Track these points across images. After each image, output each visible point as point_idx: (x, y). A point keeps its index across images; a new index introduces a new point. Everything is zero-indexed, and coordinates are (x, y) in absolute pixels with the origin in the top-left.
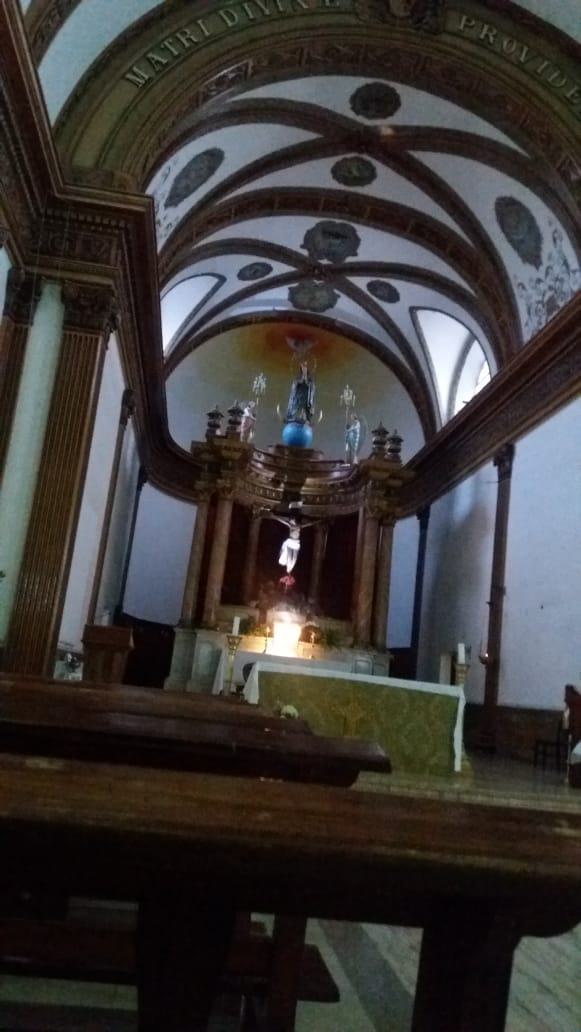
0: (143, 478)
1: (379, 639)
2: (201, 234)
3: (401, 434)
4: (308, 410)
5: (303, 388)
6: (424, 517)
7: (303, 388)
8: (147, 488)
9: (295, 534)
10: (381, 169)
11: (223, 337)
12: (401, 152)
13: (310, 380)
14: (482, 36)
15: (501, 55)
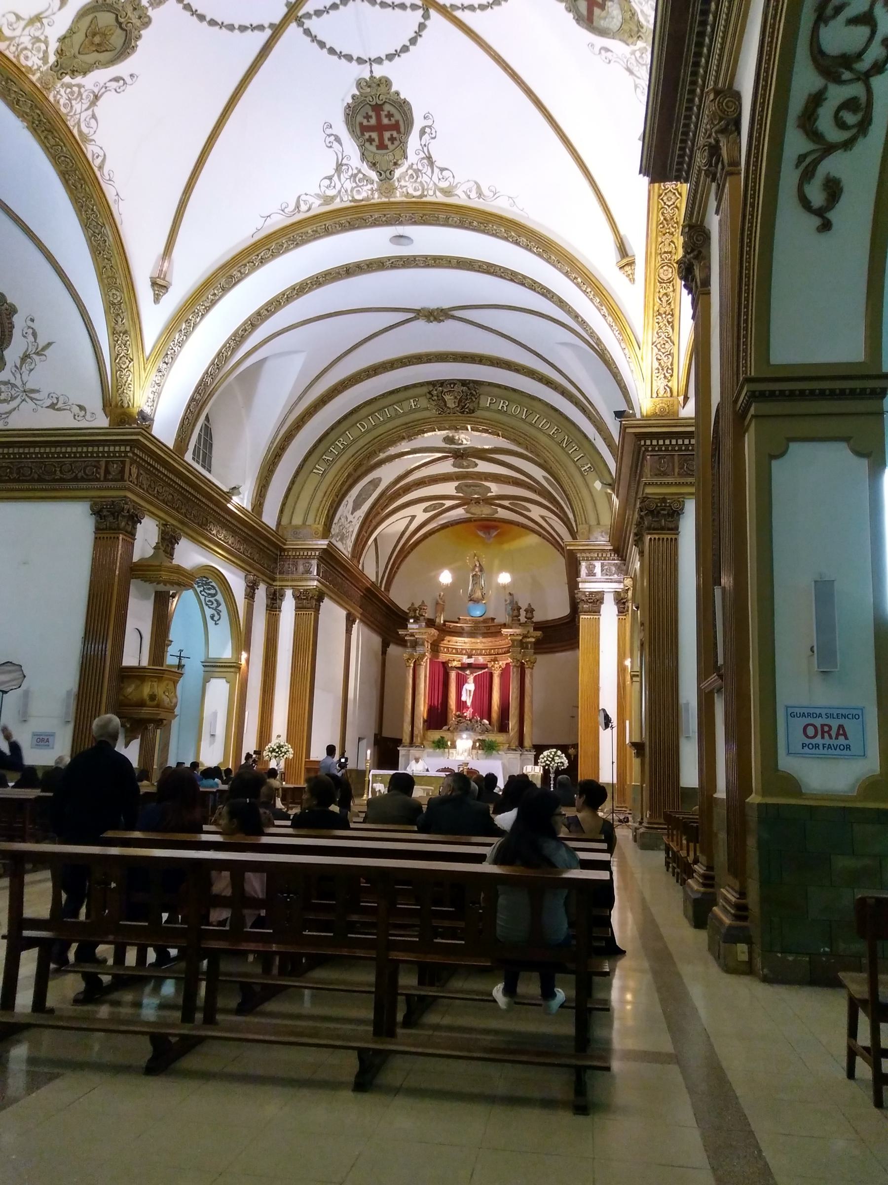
0: (385, 646)
1: (527, 743)
2: (387, 506)
9: (471, 679)
10: (477, 461)
14: (500, 408)
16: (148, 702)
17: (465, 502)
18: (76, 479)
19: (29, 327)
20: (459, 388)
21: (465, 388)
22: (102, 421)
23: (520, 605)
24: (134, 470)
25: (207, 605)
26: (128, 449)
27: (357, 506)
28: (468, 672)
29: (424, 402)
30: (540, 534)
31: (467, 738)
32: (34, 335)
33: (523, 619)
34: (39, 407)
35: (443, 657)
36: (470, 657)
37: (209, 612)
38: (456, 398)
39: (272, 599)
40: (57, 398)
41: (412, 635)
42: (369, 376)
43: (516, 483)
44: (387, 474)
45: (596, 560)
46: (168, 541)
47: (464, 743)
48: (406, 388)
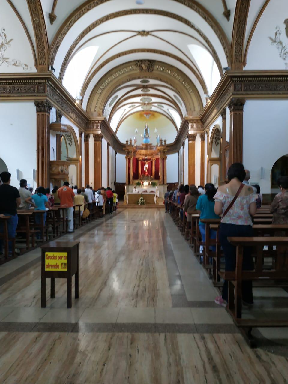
0: (116, 153)
1: (165, 183)
2: (118, 105)
3: (166, 140)
4: (148, 135)
5: (146, 130)
6: (179, 153)
7: (146, 130)
8: (118, 154)
9: (147, 163)
11: (130, 117)
12: (153, 87)
13: (148, 128)
15: (165, 73)
16: (61, 173)
17: (143, 104)
18: (26, 92)
19: (3, 33)
20: (147, 63)
21: (149, 63)
22: (34, 70)
23: (162, 139)
24: (48, 90)
25: (67, 139)
26: (46, 81)
27: (110, 106)
28: (146, 161)
29: (134, 68)
30: (165, 115)
31: (147, 182)
32: (5, 36)
33: (163, 143)
34: (9, 65)
35: (137, 157)
36: (146, 156)
37: (68, 142)
38: (146, 66)
39: (86, 138)
40: (16, 62)
41: (128, 149)
42: (117, 57)
43: (162, 97)
44: (120, 94)
45: (194, 123)
46: (59, 116)
47: (146, 183)
48: (129, 62)
